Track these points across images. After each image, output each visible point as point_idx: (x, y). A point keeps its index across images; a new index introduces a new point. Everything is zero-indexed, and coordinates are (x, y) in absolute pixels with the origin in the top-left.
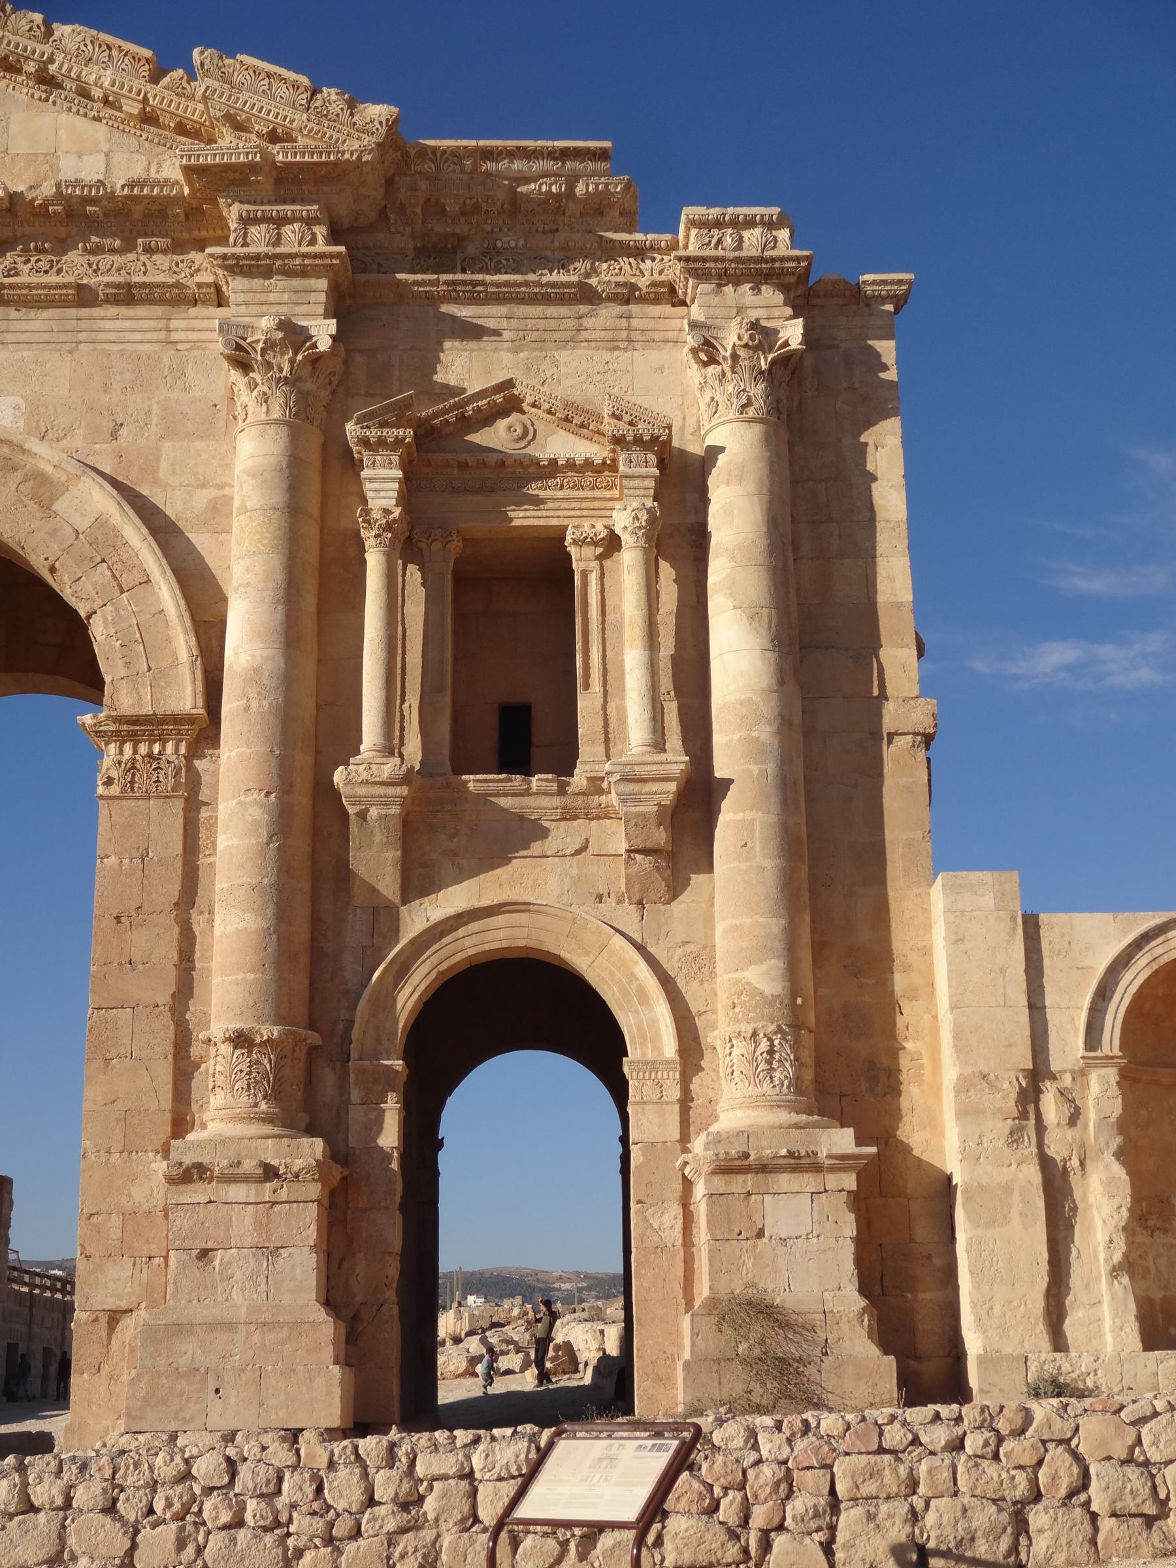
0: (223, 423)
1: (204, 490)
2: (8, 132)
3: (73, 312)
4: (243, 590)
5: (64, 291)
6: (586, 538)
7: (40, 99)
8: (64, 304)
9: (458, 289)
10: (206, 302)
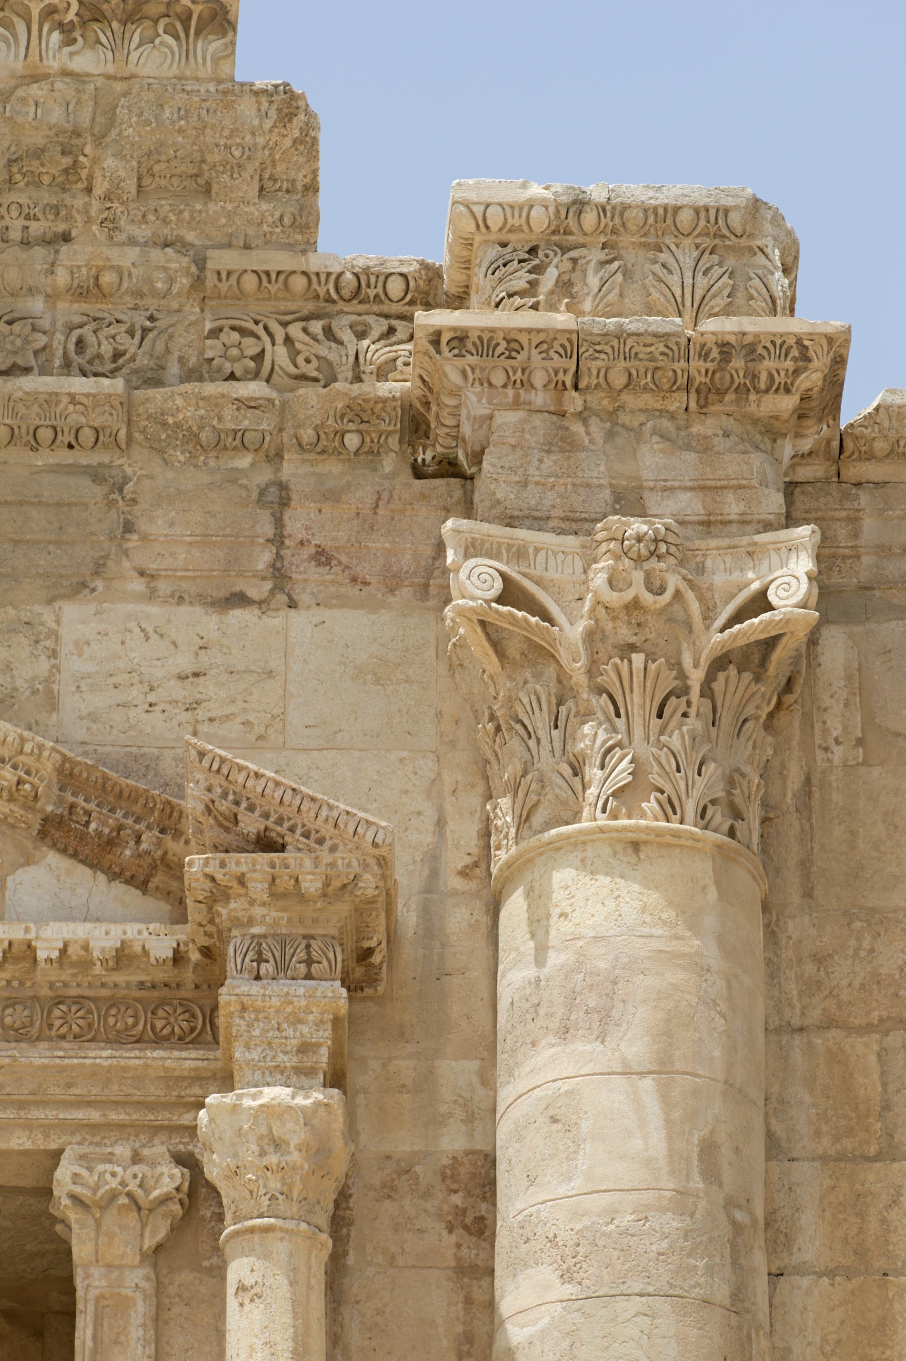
6: (113, 1196)
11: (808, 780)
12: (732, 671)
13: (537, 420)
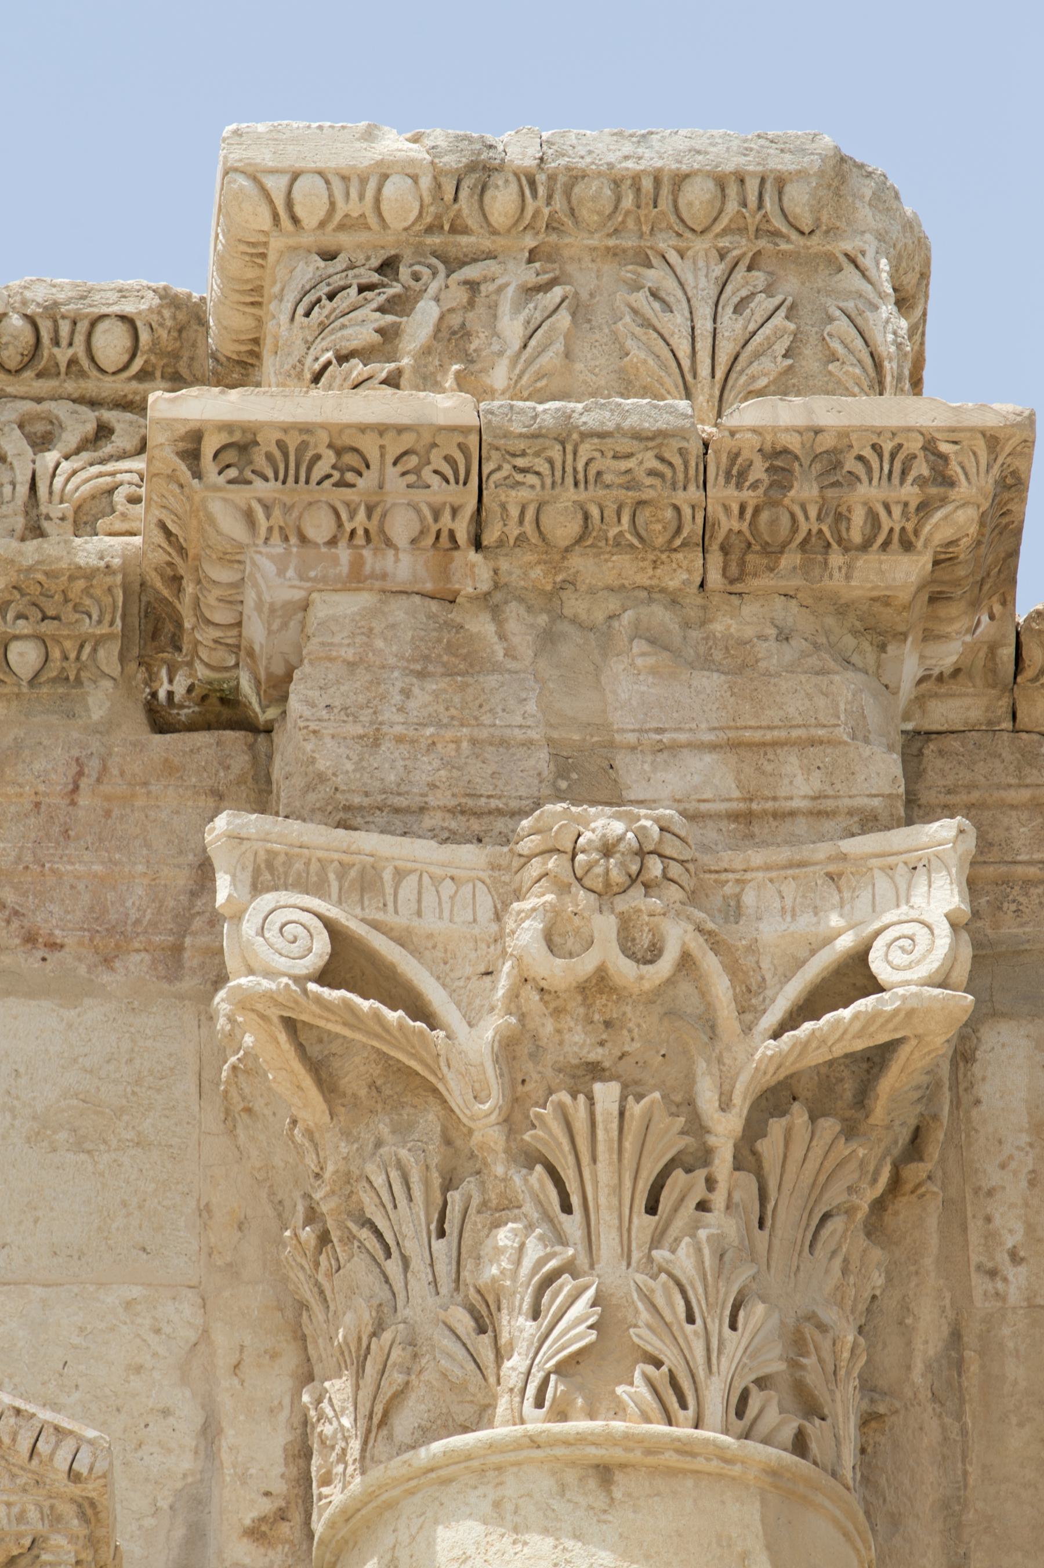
11: (956, 1336)
12: (799, 1115)
13: (399, 610)
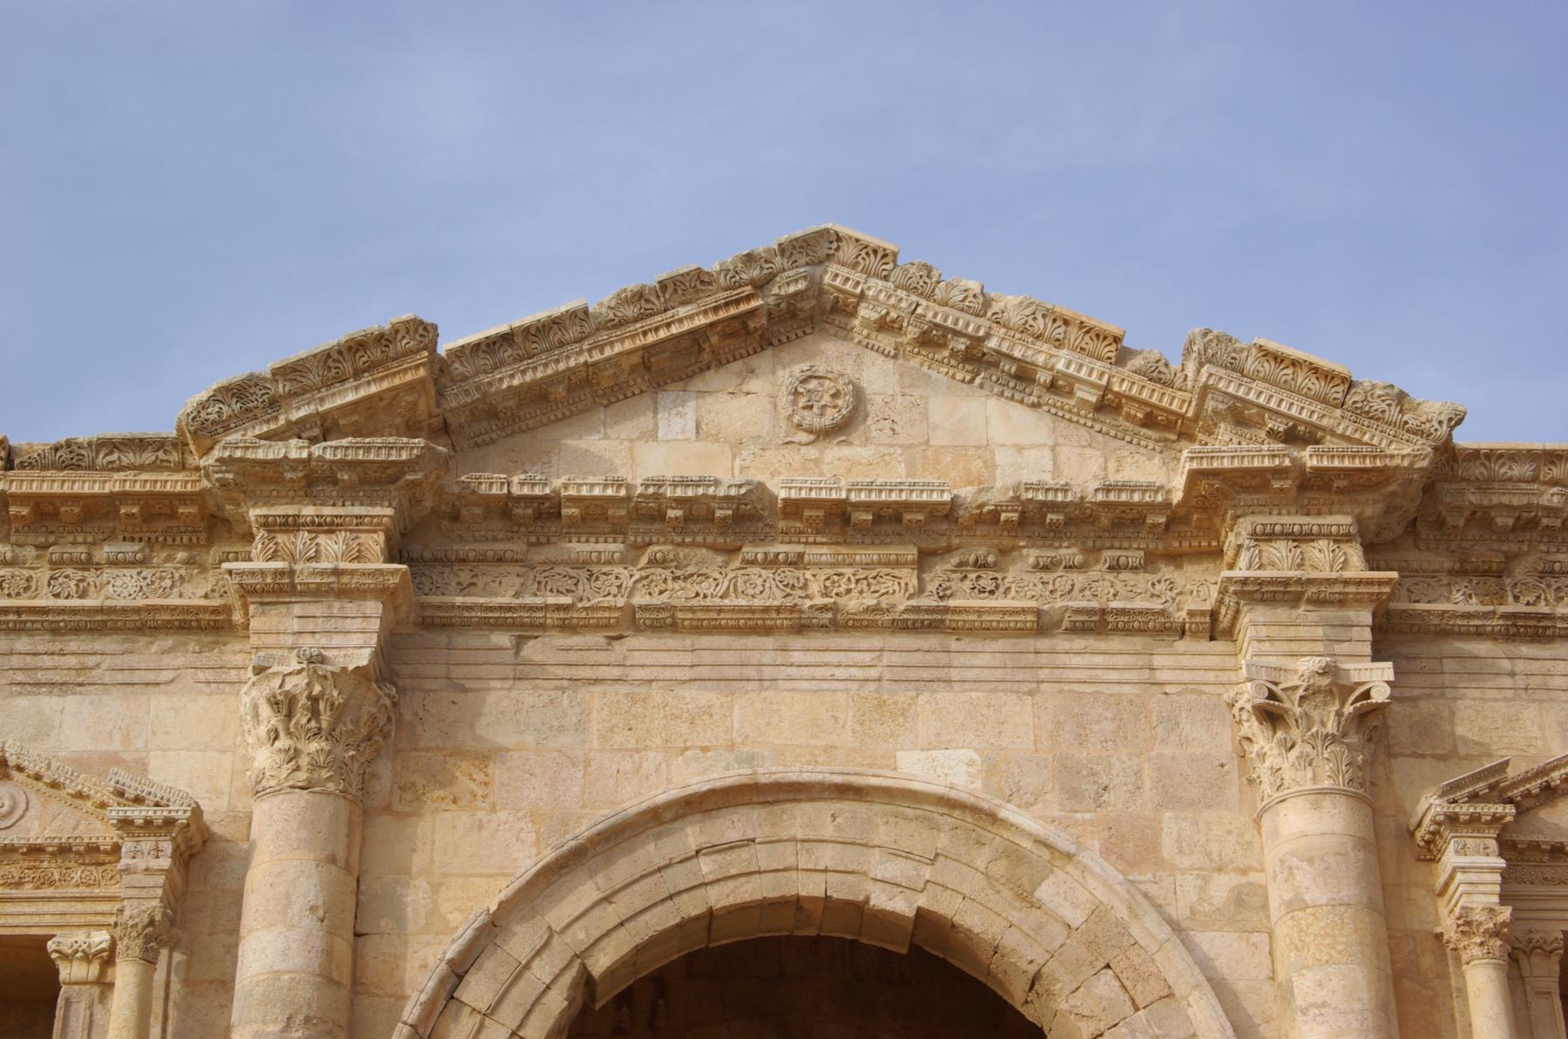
0: (1235, 789)
1: (1223, 875)
2: (927, 419)
3: (1031, 643)
4: (1316, 1011)
5: (1022, 618)
7: (963, 381)
8: (1021, 632)
9: (1520, 623)
10: (1195, 634)
